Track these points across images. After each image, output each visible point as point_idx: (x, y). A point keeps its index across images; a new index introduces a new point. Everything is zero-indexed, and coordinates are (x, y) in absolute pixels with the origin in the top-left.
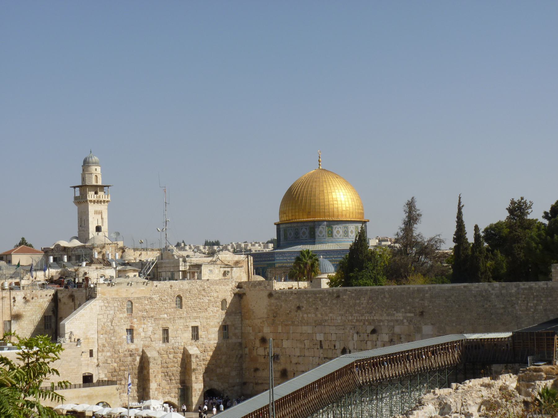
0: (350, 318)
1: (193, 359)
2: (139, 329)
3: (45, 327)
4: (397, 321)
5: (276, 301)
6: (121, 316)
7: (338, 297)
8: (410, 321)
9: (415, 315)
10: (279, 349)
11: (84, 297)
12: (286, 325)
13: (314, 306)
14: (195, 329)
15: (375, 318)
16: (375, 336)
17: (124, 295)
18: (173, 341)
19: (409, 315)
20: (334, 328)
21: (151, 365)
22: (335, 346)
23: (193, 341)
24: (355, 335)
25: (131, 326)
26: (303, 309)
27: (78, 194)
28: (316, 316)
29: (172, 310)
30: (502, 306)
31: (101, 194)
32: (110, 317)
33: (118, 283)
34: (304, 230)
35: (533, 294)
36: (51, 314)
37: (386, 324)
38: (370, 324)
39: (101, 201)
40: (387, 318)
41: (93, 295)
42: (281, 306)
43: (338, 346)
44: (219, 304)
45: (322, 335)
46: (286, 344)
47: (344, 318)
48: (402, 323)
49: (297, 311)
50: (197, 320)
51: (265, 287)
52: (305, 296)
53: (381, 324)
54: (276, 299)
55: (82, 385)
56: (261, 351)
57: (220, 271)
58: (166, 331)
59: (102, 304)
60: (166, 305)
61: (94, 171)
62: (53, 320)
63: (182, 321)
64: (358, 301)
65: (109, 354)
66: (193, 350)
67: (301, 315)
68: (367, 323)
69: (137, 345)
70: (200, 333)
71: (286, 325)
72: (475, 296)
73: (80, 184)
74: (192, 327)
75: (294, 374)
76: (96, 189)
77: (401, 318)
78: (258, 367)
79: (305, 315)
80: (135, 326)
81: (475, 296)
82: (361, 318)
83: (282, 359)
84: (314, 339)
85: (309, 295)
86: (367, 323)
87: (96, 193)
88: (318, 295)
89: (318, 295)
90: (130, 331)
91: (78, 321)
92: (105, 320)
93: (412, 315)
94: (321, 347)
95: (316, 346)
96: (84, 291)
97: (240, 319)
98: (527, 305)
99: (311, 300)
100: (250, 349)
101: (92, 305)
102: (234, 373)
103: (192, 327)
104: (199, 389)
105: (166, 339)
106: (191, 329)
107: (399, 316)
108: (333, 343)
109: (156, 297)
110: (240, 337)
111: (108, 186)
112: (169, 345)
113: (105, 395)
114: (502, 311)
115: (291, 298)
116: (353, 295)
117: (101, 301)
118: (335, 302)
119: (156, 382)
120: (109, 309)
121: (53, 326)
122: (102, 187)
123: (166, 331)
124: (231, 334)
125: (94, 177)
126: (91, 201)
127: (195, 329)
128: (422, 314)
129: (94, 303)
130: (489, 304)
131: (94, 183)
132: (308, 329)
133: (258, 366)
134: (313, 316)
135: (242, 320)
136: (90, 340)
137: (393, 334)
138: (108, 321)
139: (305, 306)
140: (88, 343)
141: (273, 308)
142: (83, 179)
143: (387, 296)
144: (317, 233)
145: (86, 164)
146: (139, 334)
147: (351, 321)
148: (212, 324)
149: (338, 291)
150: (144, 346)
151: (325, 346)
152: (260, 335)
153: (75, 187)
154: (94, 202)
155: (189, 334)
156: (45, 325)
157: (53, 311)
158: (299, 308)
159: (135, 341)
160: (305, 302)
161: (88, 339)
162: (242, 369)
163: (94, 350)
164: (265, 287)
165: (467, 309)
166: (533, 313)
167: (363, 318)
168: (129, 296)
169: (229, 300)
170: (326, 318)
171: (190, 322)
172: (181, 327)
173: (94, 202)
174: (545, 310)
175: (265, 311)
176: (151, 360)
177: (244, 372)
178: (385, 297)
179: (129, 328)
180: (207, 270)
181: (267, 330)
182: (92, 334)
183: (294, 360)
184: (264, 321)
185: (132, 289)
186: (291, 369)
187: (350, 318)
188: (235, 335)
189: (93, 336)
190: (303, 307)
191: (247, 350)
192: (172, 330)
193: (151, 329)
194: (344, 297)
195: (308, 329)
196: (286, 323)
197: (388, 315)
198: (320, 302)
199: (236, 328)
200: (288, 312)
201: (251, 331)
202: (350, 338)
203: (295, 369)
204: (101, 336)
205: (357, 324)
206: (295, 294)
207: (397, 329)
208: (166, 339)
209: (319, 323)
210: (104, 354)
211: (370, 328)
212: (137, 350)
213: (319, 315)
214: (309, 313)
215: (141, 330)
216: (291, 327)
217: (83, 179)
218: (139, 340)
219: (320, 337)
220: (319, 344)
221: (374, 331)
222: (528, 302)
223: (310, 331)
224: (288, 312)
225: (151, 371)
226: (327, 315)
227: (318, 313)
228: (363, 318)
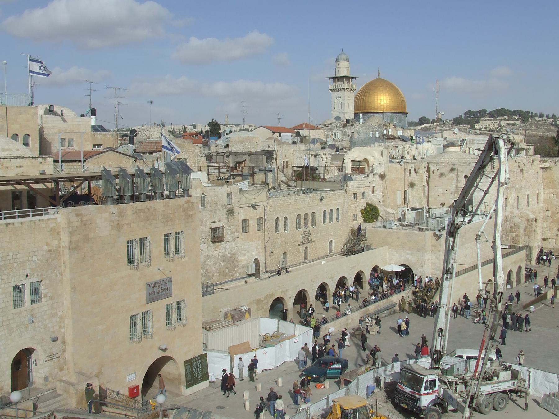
62: (427, 189)
73: (334, 76)
100: (553, 213)
111: (355, 78)
124: (539, 201)
153: (330, 78)
201: (555, 198)
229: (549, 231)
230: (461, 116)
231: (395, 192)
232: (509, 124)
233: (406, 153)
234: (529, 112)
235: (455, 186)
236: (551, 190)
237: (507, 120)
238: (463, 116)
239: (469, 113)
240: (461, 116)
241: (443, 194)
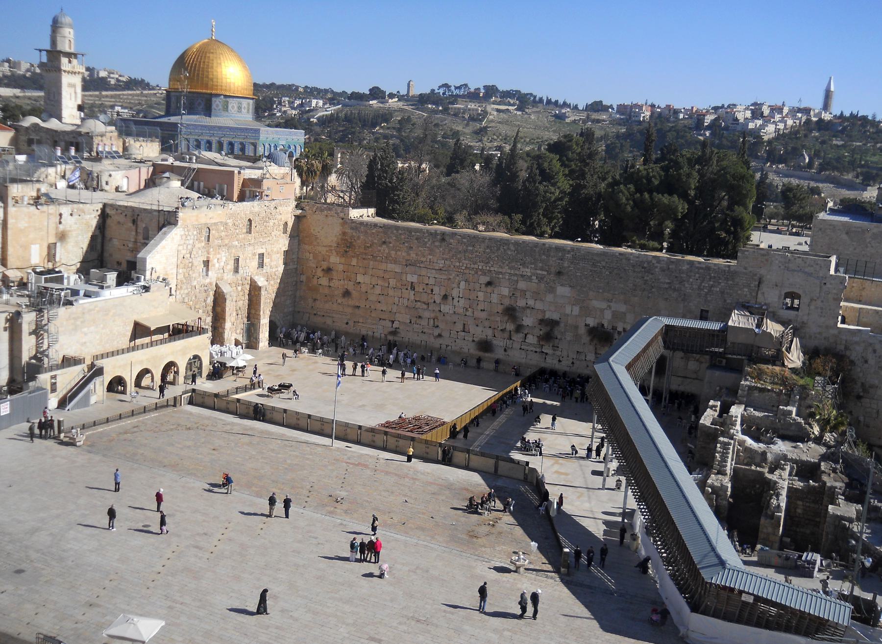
0: (458, 264)
1: (263, 292)
2: (214, 261)
4: (522, 276)
7: (443, 240)
8: (541, 279)
9: (549, 273)
10: (351, 283)
15: (492, 269)
16: (489, 289)
17: (203, 221)
19: (539, 272)
20: (434, 271)
21: (227, 301)
22: (432, 290)
24: (463, 284)
27: (45, 59)
28: (409, 254)
30: (667, 281)
31: (75, 61)
32: (190, 247)
34: (199, 101)
35: (710, 274)
36: (98, 233)
37: (507, 277)
38: (484, 274)
39: (75, 73)
40: (509, 271)
41: (172, 221)
42: (359, 238)
43: (436, 290)
45: (416, 277)
46: (360, 278)
47: (448, 263)
48: (529, 279)
49: (381, 246)
51: (337, 213)
53: (501, 276)
54: (352, 228)
56: (324, 281)
61: (67, 34)
63: (251, 248)
64: (471, 248)
65: (186, 291)
66: (261, 282)
67: (387, 251)
68: (480, 273)
72: (633, 266)
73: (49, 48)
76: (69, 55)
77: (529, 274)
79: (393, 253)
81: (633, 266)
82: (472, 266)
83: (354, 293)
84: (404, 278)
86: (480, 273)
87: (70, 62)
90: (207, 263)
93: (545, 273)
94: (413, 288)
98: (701, 285)
102: (288, 302)
105: (236, 270)
107: (528, 272)
108: (431, 287)
109: (230, 222)
112: (239, 276)
114: (666, 286)
116: (465, 240)
118: (437, 244)
121: (99, 247)
122: (76, 55)
125: (67, 42)
126: (65, 71)
127: (261, 256)
128: (559, 273)
130: (651, 276)
131: (67, 50)
132: (398, 269)
135: (299, 244)
137: (516, 289)
142: (54, 42)
143: (512, 248)
144: (214, 106)
145: (56, 26)
146: (214, 265)
147: (458, 267)
148: (275, 249)
149: (443, 234)
150: (218, 279)
151: (419, 288)
152: (325, 265)
153: (40, 51)
154: (69, 72)
155: (255, 263)
159: (210, 273)
162: (295, 297)
164: (337, 213)
165: (621, 278)
166: (707, 294)
167: (476, 266)
168: (208, 222)
169: (290, 225)
170: (424, 259)
173: (69, 72)
174: (722, 293)
176: (227, 297)
178: (509, 249)
181: (334, 259)
185: (211, 213)
187: (458, 264)
191: (303, 278)
193: (224, 259)
194: (452, 241)
195: (398, 269)
197: (510, 268)
201: (311, 258)
202: (455, 285)
204: (181, 271)
205: (467, 271)
207: (522, 285)
208: (236, 270)
209: (409, 264)
210: (182, 292)
211: (484, 279)
212: (211, 284)
215: (216, 261)
216: (371, 263)
217: (54, 42)
219: (413, 278)
221: (489, 284)
222: (703, 281)
225: (227, 309)
226: (424, 256)
228: (476, 266)
230: (433, 91)
231: (26, 248)
232: (498, 111)
233: (104, 184)
234: (531, 94)
235: (133, 240)
236: (307, 247)
237: (499, 104)
238: (437, 91)
239: (446, 86)
240: (433, 91)
241: (119, 250)
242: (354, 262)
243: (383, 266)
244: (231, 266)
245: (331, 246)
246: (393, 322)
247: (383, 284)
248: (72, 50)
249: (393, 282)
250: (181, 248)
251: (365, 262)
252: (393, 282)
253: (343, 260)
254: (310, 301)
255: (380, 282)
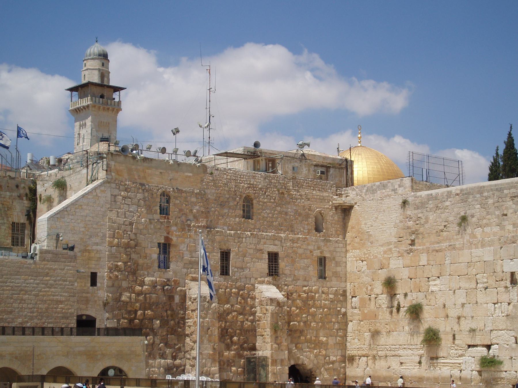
3: (13, 241)
5: (416, 211)
6: (151, 217)
10: (421, 295)
11: (84, 182)
12: (437, 251)
13: (497, 213)
14: (273, 258)
18: (237, 274)
23: (270, 279)
25: (167, 238)
26: (474, 219)
29: (237, 219)
33: (145, 159)
36: (23, 219)
42: (427, 219)
44: (312, 220)
46: (435, 286)
50: (277, 242)
51: (394, 190)
52: (478, 196)
55: (75, 331)
57: (309, 170)
58: (225, 256)
59: (116, 192)
60: (226, 211)
69: (175, 272)
70: (282, 264)
71: (437, 251)
74: (270, 254)
75: (454, 335)
78: (380, 329)
80: (174, 239)
84: (498, 269)
85: (486, 194)
88: (506, 192)
89: (506, 192)
90: (165, 248)
91: (71, 217)
92: (121, 220)
95: (502, 282)
96: (85, 171)
97: (344, 250)
99: (491, 201)
100: (362, 300)
101: (98, 191)
103: (270, 254)
104: (282, 361)
105: (225, 271)
106: (267, 256)
110: (343, 279)
113: (120, 355)
115: (448, 203)
117: (113, 185)
119: (210, 341)
120: (128, 201)
123: (225, 256)
124: (328, 273)
127: (273, 258)
129: (103, 188)
132: (486, 254)
133: (379, 327)
134: (496, 229)
136: (93, 255)
138: (127, 223)
139: (477, 215)
140: (90, 259)
141: (411, 223)
148: (300, 251)
152: (383, 274)
155: (264, 265)
156: (13, 238)
157: (28, 215)
158: (464, 219)
160: (478, 206)
161: (89, 251)
163: (98, 274)
164: (394, 190)
171: (265, 243)
172: (251, 251)
175: (394, 231)
177: (349, 339)
179: (162, 241)
180: (291, 167)
182: (97, 244)
183: (453, 313)
184: (390, 250)
186: (448, 329)
188: (336, 275)
189: (99, 248)
190: (473, 216)
192: (237, 254)
195: (486, 254)
196: (436, 246)
198: (511, 203)
199: (338, 264)
200: (442, 227)
201: (365, 268)
203: (456, 328)
206: (457, 195)
208: (225, 271)
213: (510, 227)
214: (487, 225)
216: (448, 253)
218: (181, 264)
220: (509, 280)
223: (488, 257)
224: (442, 227)
227: (506, 223)
229: (356, 340)
242: (424, 259)
243: (465, 256)
244: (216, 259)
245: (389, 243)
246: (489, 347)
247: (467, 285)
248: (105, 83)
249: (482, 278)
250: (113, 215)
251: (440, 253)
252: (482, 278)
253: (408, 259)
254: (367, 335)
255: (464, 284)
